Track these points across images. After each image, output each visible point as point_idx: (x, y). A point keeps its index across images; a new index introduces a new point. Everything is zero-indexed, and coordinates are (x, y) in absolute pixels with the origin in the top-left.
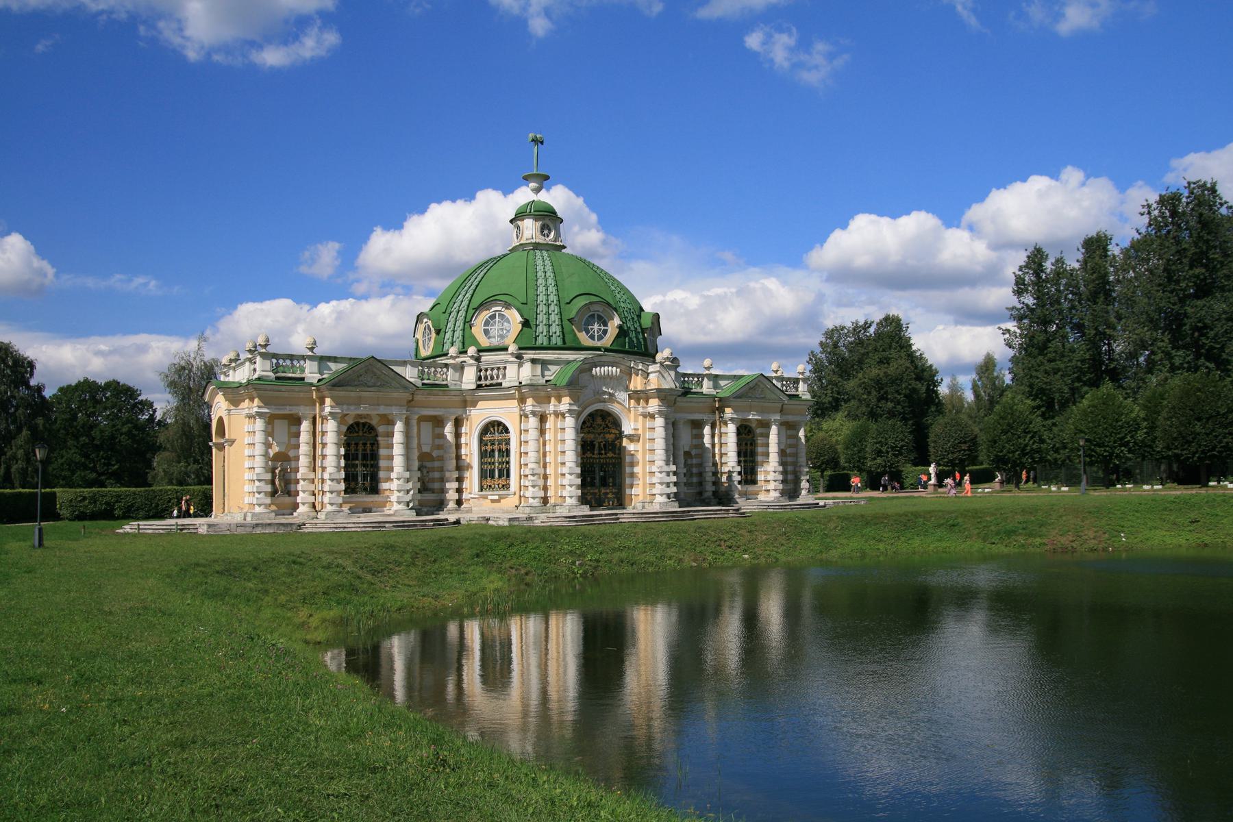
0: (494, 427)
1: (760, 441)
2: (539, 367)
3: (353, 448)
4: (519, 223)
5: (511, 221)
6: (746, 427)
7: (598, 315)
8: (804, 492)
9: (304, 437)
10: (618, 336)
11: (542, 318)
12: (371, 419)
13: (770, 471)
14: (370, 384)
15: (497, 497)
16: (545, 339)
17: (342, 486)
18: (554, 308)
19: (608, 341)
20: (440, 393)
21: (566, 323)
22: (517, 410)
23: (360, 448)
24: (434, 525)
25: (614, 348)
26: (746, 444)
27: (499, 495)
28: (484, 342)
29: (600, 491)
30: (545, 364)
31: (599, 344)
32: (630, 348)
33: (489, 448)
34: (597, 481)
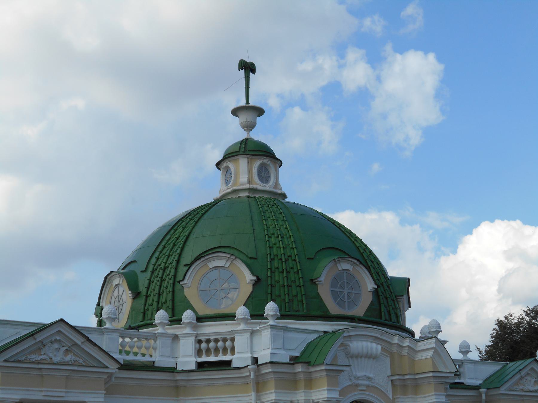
4: (231, 165)
5: (218, 165)
28: (203, 311)
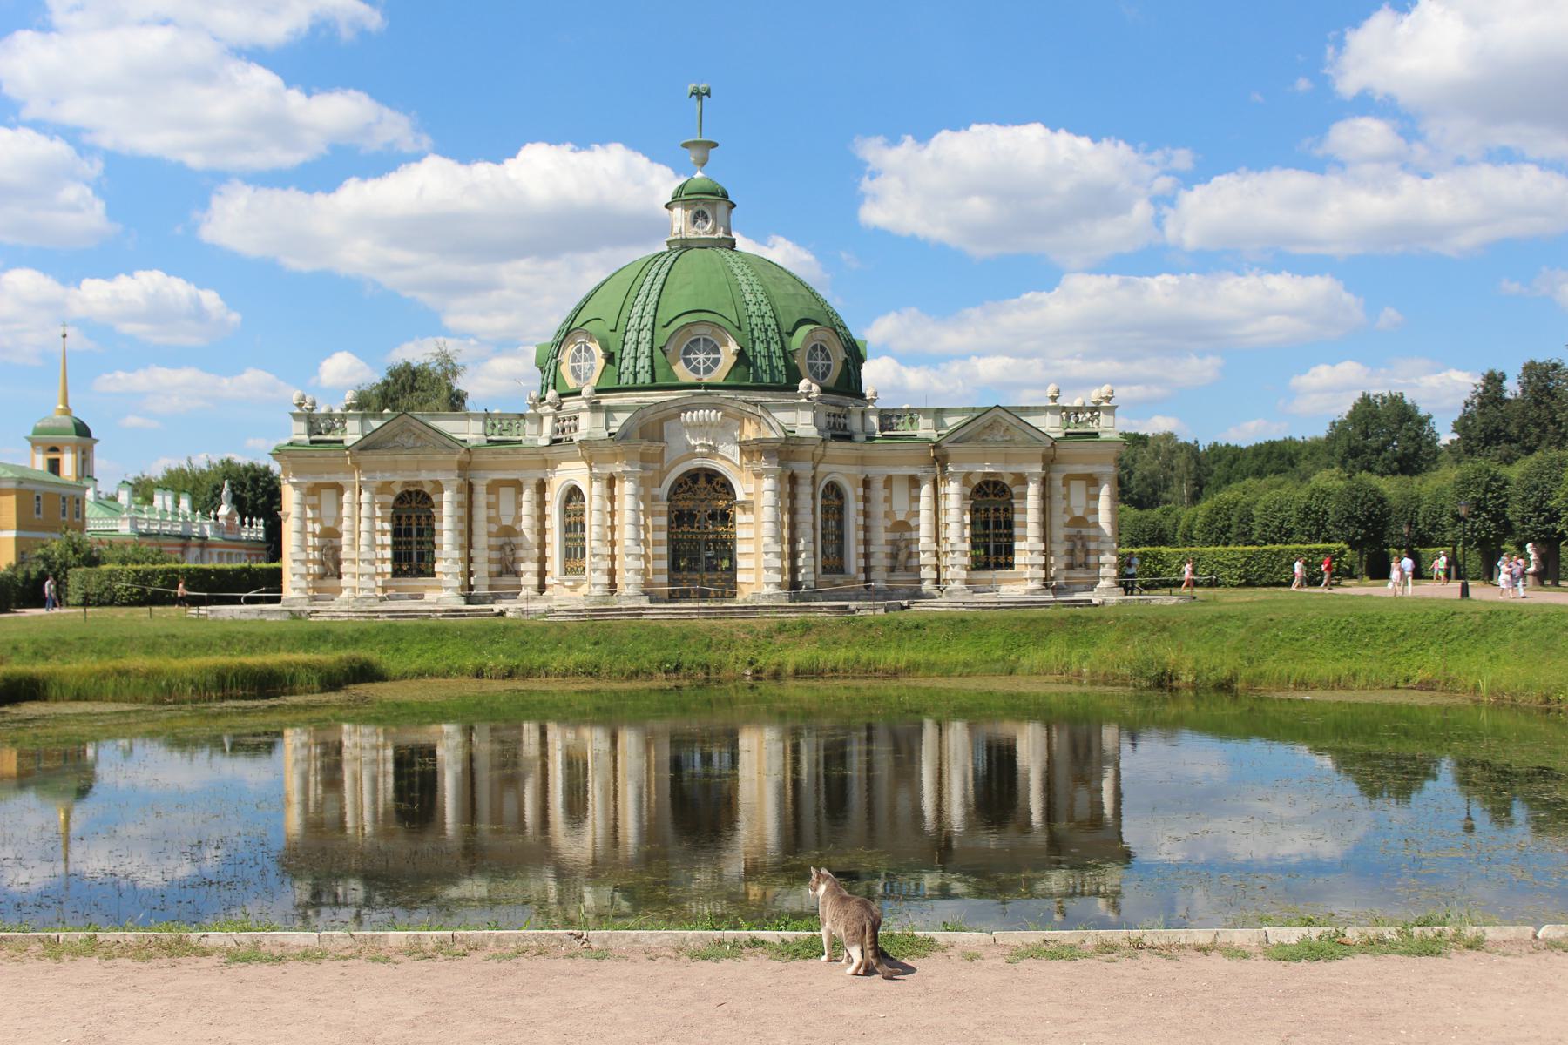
0: (573, 494)
1: (1017, 504)
2: (602, 416)
3: (404, 522)
6: (996, 484)
7: (704, 339)
8: (1103, 583)
9: (346, 511)
10: (736, 365)
11: (629, 348)
12: (422, 486)
13: (1027, 547)
14: (409, 445)
15: (571, 584)
16: (631, 377)
17: (388, 567)
18: (646, 334)
19: (719, 375)
20: (510, 452)
21: (658, 353)
22: (587, 471)
23: (414, 520)
24: (442, 616)
25: (725, 383)
26: (996, 510)
27: (574, 580)
28: (572, 384)
29: (702, 577)
30: (609, 410)
31: (706, 379)
32: (754, 381)
33: (572, 519)
34: (702, 565)
